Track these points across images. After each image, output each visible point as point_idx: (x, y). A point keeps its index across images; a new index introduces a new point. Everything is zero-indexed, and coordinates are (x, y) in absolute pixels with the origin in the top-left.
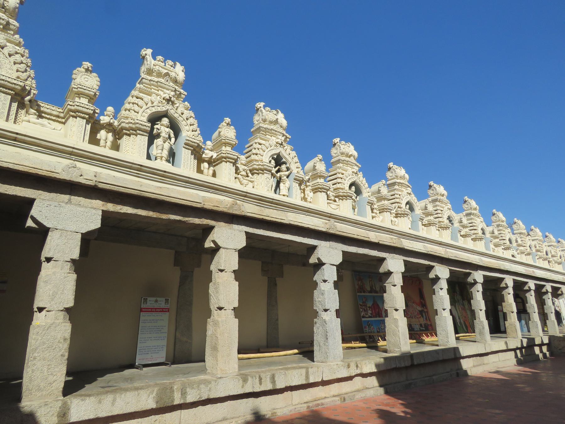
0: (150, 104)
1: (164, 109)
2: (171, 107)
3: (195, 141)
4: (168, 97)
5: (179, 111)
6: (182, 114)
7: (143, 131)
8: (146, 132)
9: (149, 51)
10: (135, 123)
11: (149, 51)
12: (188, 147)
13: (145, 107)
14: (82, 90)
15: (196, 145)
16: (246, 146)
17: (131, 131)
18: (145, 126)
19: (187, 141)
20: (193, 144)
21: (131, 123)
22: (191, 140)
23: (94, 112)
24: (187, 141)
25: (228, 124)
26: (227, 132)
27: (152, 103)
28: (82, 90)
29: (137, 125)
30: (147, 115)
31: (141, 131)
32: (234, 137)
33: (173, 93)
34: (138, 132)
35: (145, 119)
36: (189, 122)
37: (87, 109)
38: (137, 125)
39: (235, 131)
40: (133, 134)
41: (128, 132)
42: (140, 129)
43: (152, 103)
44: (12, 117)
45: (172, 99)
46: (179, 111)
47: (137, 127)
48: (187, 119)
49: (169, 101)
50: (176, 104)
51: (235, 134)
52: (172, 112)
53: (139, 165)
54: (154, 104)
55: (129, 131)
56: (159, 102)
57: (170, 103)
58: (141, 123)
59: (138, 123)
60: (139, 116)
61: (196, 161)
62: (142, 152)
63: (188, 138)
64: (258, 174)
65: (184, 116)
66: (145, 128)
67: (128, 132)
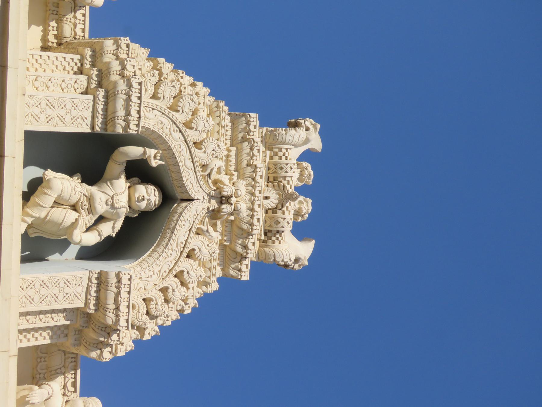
3: (123, 308)
4: (228, 190)
5: (196, 242)
6: (188, 256)
7: (105, 110)
8: (105, 123)
9: (316, 143)
11: (316, 143)
12: (94, 289)
15: (110, 319)
17: (94, 73)
18: (128, 114)
19: (113, 280)
20: (111, 305)
21: (124, 68)
22: (124, 294)
24: (113, 280)
29: (122, 86)
31: (106, 104)
34: (101, 93)
36: (172, 282)
38: (122, 86)
41: (87, 66)
42: (109, 97)
45: (226, 208)
46: (196, 242)
47: (115, 83)
48: (179, 275)
50: (214, 226)
52: (189, 217)
54: (196, 152)
55: (93, 65)
56: (204, 166)
57: (214, 205)
58: (134, 99)
60: (146, 98)
61: (44, 339)
62: (37, 111)
63: (125, 281)
65: (185, 264)
66: (121, 112)
67: (87, 66)
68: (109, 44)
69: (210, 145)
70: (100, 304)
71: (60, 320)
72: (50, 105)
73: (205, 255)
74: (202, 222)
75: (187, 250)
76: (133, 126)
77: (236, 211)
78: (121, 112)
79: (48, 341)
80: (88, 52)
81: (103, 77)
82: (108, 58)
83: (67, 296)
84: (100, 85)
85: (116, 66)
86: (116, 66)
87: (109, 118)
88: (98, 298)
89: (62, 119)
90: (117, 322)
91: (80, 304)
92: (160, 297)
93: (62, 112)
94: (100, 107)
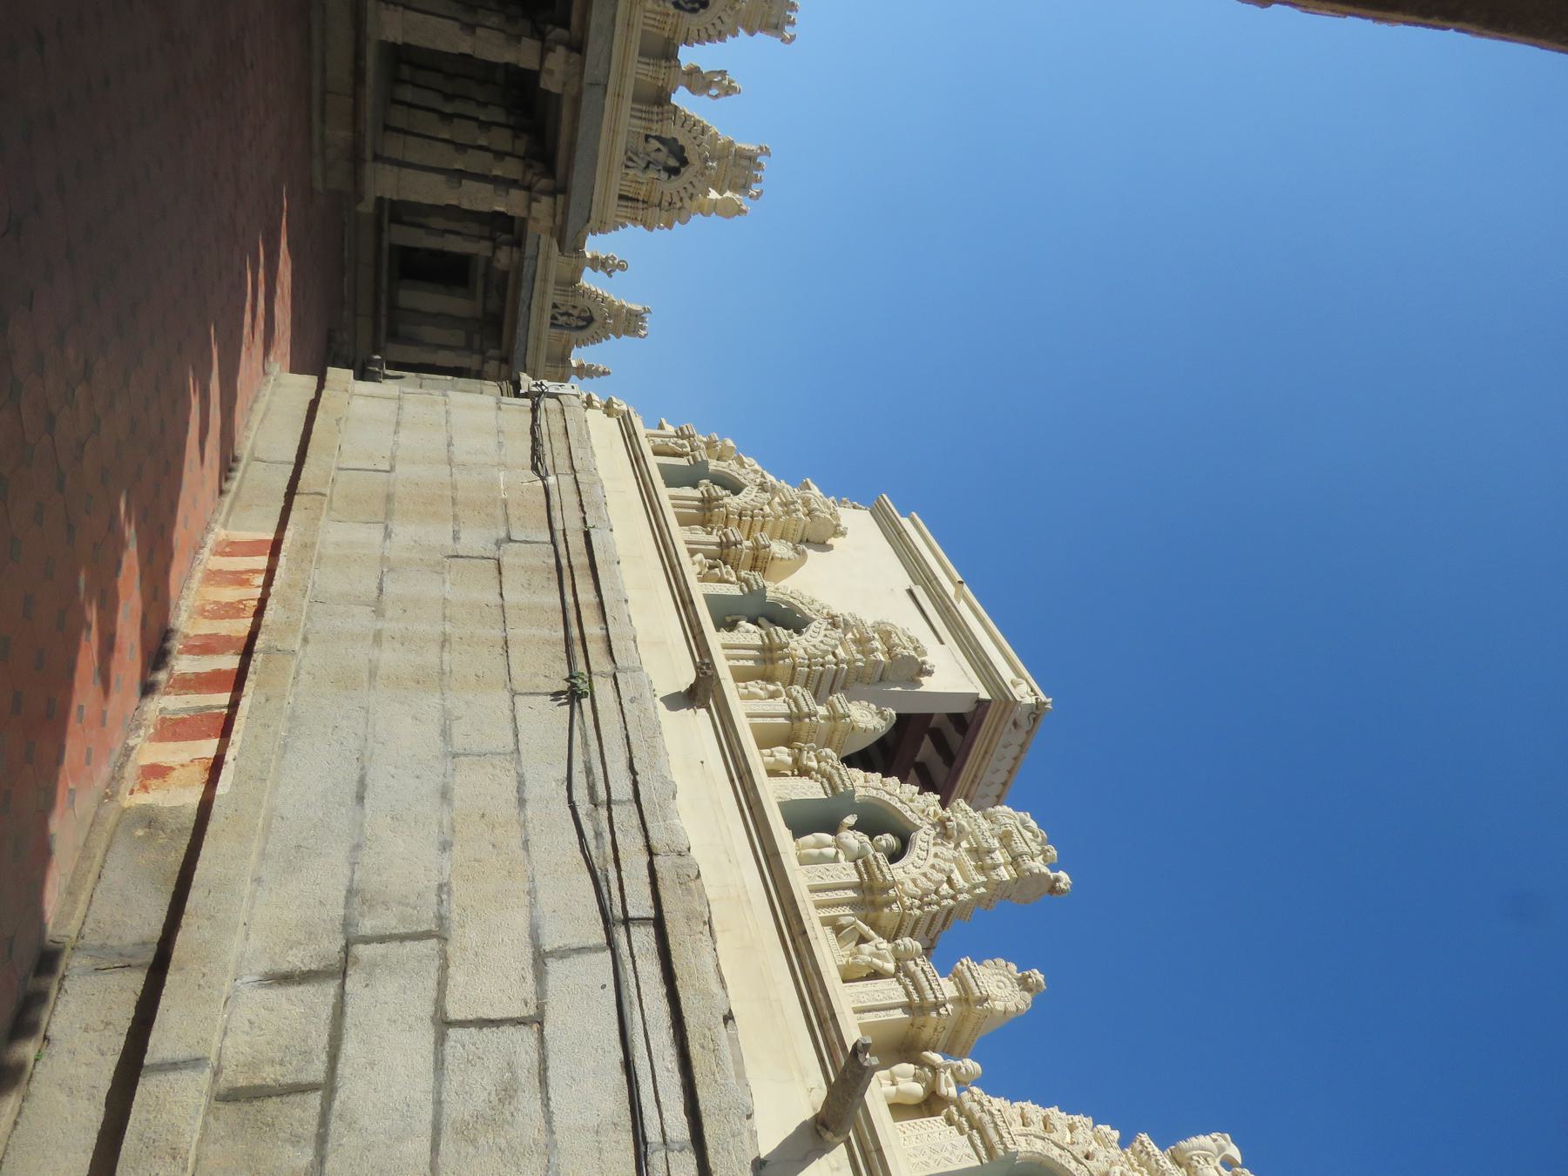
0: (1078, 1151)
7: (983, 1142)
13: (1054, 1136)
17: (963, 1120)
18: (1001, 1137)
23: (937, 1006)
29: (987, 1118)
30: (1038, 1146)
31: (982, 1138)
38: (987, 1118)
44: (824, 896)
59: (991, 1114)
66: (996, 1139)
68: (965, 1095)
69: (1101, 1154)
72: (934, 1151)
78: (996, 1139)
80: (953, 1108)
82: (968, 1104)
84: (972, 1127)
86: (976, 1107)
87: (990, 1149)
89: (949, 1161)
93: (947, 1155)
94: (978, 1142)
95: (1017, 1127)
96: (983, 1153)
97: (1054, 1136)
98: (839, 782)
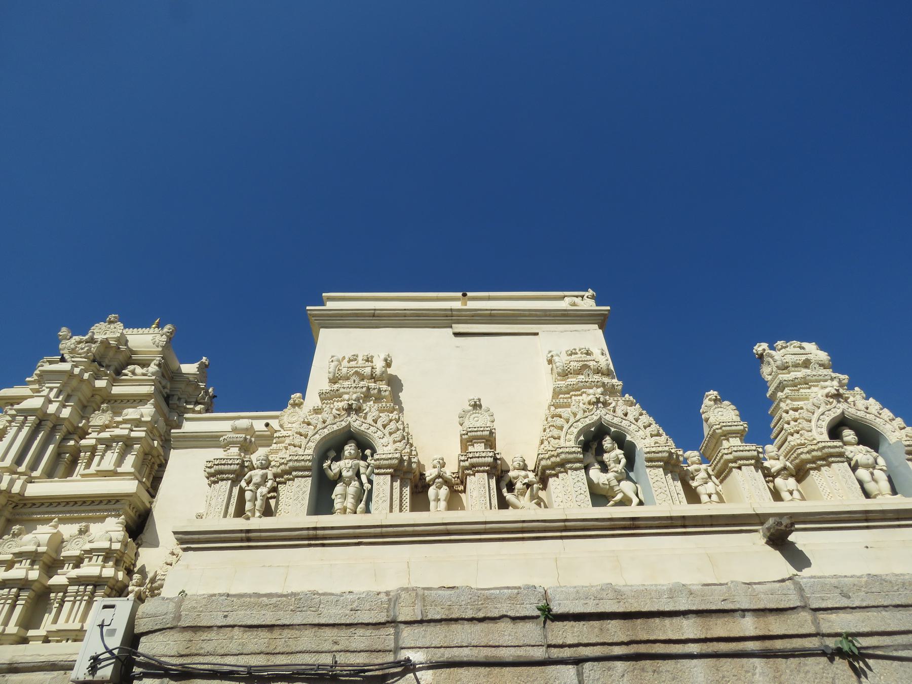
0: (320, 426)
1: (344, 424)
2: (355, 417)
3: (390, 456)
10: (558, 455)
12: (383, 471)
13: (310, 434)
14: (473, 434)
16: (772, 425)
17: (286, 477)
21: (283, 463)
25: (716, 400)
26: (720, 414)
27: (575, 415)
28: (473, 434)
29: (291, 464)
30: (312, 445)
32: (738, 419)
33: (600, 390)
34: (294, 473)
35: (310, 452)
37: (224, 464)
39: (733, 407)
40: (289, 480)
43: (324, 422)
46: (370, 420)
48: (384, 426)
49: (349, 409)
51: (737, 412)
53: (308, 529)
56: (335, 417)
59: (290, 460)
60: (300, 451)
61: (407, 491)
64: (556, 475)
65: (379, 424)
70: (389, 467)
71: (397, 484)
73: (376, 413)
74: (361, 417)
75: (373, 423)
76: (309, 458)
77: (357, 399)
79: (408, 489)
81: (289, 472)
83: (385, 483)
85: (283, 467)
86: (283, 467)
88: (387, 468)
89: (304, 492)
90: (396, 458)
91: (389, 477)
92: (394, 435)
94: (300, 473)
95: (300, 451)
96: (307, 473)
97: (310, 434)
98: (574, 455)
